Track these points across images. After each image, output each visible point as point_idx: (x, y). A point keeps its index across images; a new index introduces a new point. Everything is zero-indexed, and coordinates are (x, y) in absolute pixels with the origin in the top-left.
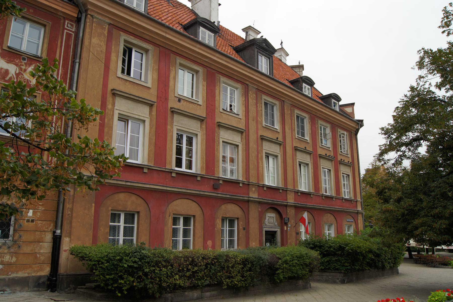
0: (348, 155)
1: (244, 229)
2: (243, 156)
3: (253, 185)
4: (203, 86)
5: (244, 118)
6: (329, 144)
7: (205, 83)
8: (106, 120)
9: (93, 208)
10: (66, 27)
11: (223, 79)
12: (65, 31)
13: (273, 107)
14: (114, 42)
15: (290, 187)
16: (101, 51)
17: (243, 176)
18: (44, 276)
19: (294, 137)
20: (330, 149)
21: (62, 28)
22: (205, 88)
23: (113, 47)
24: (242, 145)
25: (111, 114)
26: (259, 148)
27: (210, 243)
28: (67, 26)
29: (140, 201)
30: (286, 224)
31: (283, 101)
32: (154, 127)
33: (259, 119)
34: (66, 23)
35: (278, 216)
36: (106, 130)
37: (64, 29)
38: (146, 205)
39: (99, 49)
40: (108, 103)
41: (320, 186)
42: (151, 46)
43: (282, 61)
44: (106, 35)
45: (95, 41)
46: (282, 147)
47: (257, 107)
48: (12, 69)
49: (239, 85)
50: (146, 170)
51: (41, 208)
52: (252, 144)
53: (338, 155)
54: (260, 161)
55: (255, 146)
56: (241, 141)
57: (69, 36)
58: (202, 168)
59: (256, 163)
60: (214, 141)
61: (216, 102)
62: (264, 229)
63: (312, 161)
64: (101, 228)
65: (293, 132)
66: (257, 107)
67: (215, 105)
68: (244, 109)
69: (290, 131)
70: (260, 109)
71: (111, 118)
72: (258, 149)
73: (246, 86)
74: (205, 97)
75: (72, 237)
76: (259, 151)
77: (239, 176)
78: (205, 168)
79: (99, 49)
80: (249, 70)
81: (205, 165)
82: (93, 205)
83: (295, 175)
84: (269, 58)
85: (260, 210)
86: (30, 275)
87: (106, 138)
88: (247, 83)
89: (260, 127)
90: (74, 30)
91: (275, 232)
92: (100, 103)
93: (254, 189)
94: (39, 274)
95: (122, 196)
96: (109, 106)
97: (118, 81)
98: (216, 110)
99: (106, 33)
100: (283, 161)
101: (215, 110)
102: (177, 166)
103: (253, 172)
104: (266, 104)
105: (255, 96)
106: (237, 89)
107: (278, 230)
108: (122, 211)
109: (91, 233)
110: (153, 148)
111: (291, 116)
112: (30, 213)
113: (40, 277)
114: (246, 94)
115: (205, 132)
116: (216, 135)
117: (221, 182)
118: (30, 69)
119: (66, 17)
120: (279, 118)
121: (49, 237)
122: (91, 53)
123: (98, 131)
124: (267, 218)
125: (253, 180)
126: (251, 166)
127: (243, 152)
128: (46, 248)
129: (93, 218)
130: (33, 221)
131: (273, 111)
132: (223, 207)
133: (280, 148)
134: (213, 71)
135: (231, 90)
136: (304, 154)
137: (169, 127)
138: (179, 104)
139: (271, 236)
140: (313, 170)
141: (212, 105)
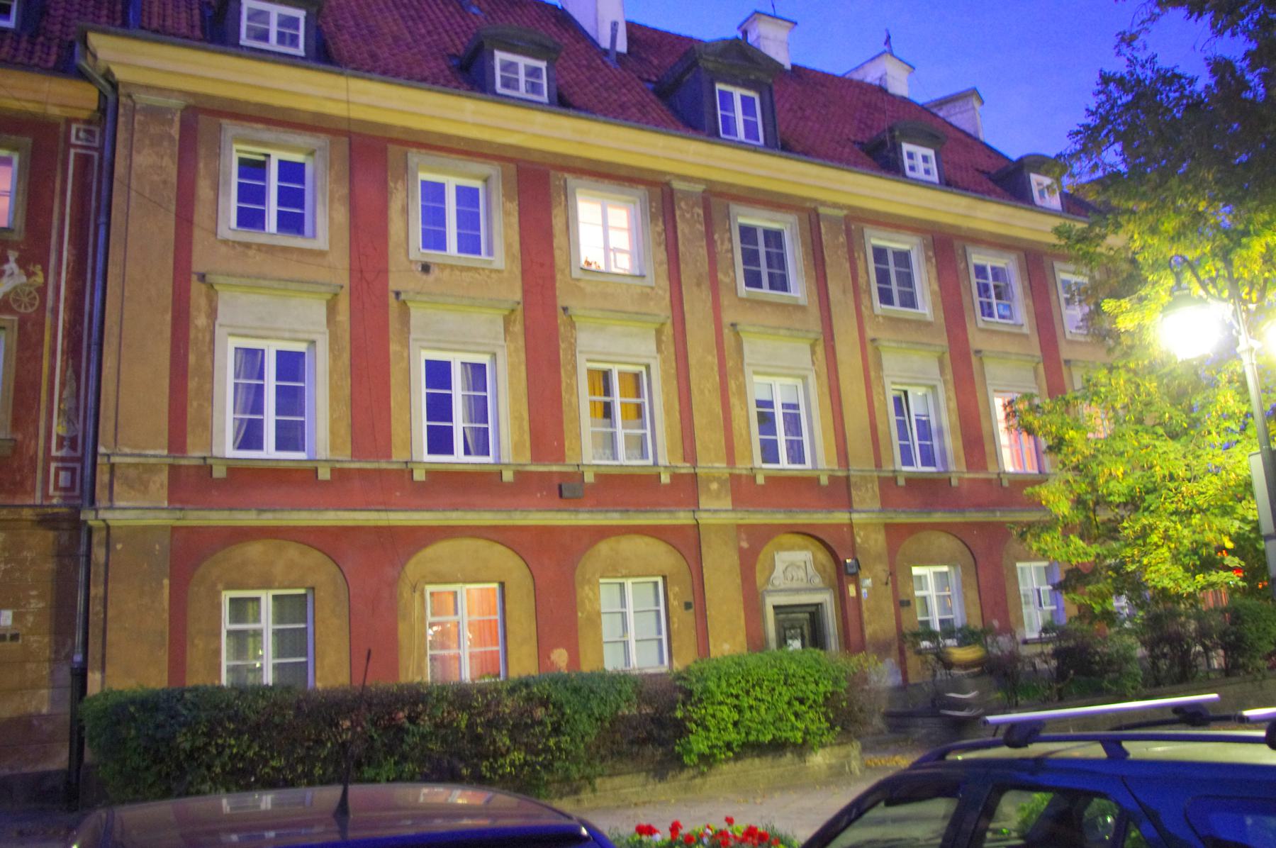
1: (688, 606)
4: (507, 214)
5: (665, 283)
7: (513, 207)
8: (192, 359)
9: (166, 591)
10: (73, 140)
12: (72, 151)
14: (202, 151)
16: (165, 182)
17: (671, 452)
18: (57, 773)
20: (1026, 330)
21: (62, 145)
22: (515, 220)
23: (201, 165)
24: (664, 361)
25: (208, 338)
26: (730, 364)
28: (77, 137)
29: (315, 557)
30: (855, 578)
32: (346, 356)
33: (721, 276)
34: (74, 132)
36: (192, 384)
37: (69, 145)
38: (334, 568)
39: (156, 178)
40: (193, 312)
42: (322, 136)
43: (891, 90)
44: (177, 137)
45: (143, 159)
47: (711, 244)
51: (35, 605)
54: (734, 401)
55: (712, 359)
56: (659, 350)
57: (84, 162)
58: (517, 447)
59: (718, 409)
60: (555, 365)
61: (557, 253)
62: (771, 601)
63: (949, 377)
64: (196, 641)
66: (711, 244)
67: (552, 266)
68: (662, 255)
70: (727, 245)
71: (205, 349)
74: (516, 246)
75: (109, 670)
78: (528, 444)
79: (156, 178)
81: (527, 437)
82: (166, 582)
85: (745, 545)
86: (16, 772)
87: (195, 404)
89: (725, 300)
90: (96, 144)
92: (168, 317)
94: (40, 768)
95: (255, 550)
96: (200, 321)
97: (224, 249)
98: (559, 277)
99: (175, 131)
100: (826, 390)
102: (432, 451)
105: (701, 212)
107: (825, 598)
109: (164, 656)
110: (345, 410)
111: (851, 252)
113: (45, 775)
115: (521, 343)
116: (562, 346)
120: (801, 265)
122: (133, 194)
123: (167, 391)
126: (699, 420)
129: (166, 616)
130: (15, 637)
137: (394, 347)
138: (424, 277)
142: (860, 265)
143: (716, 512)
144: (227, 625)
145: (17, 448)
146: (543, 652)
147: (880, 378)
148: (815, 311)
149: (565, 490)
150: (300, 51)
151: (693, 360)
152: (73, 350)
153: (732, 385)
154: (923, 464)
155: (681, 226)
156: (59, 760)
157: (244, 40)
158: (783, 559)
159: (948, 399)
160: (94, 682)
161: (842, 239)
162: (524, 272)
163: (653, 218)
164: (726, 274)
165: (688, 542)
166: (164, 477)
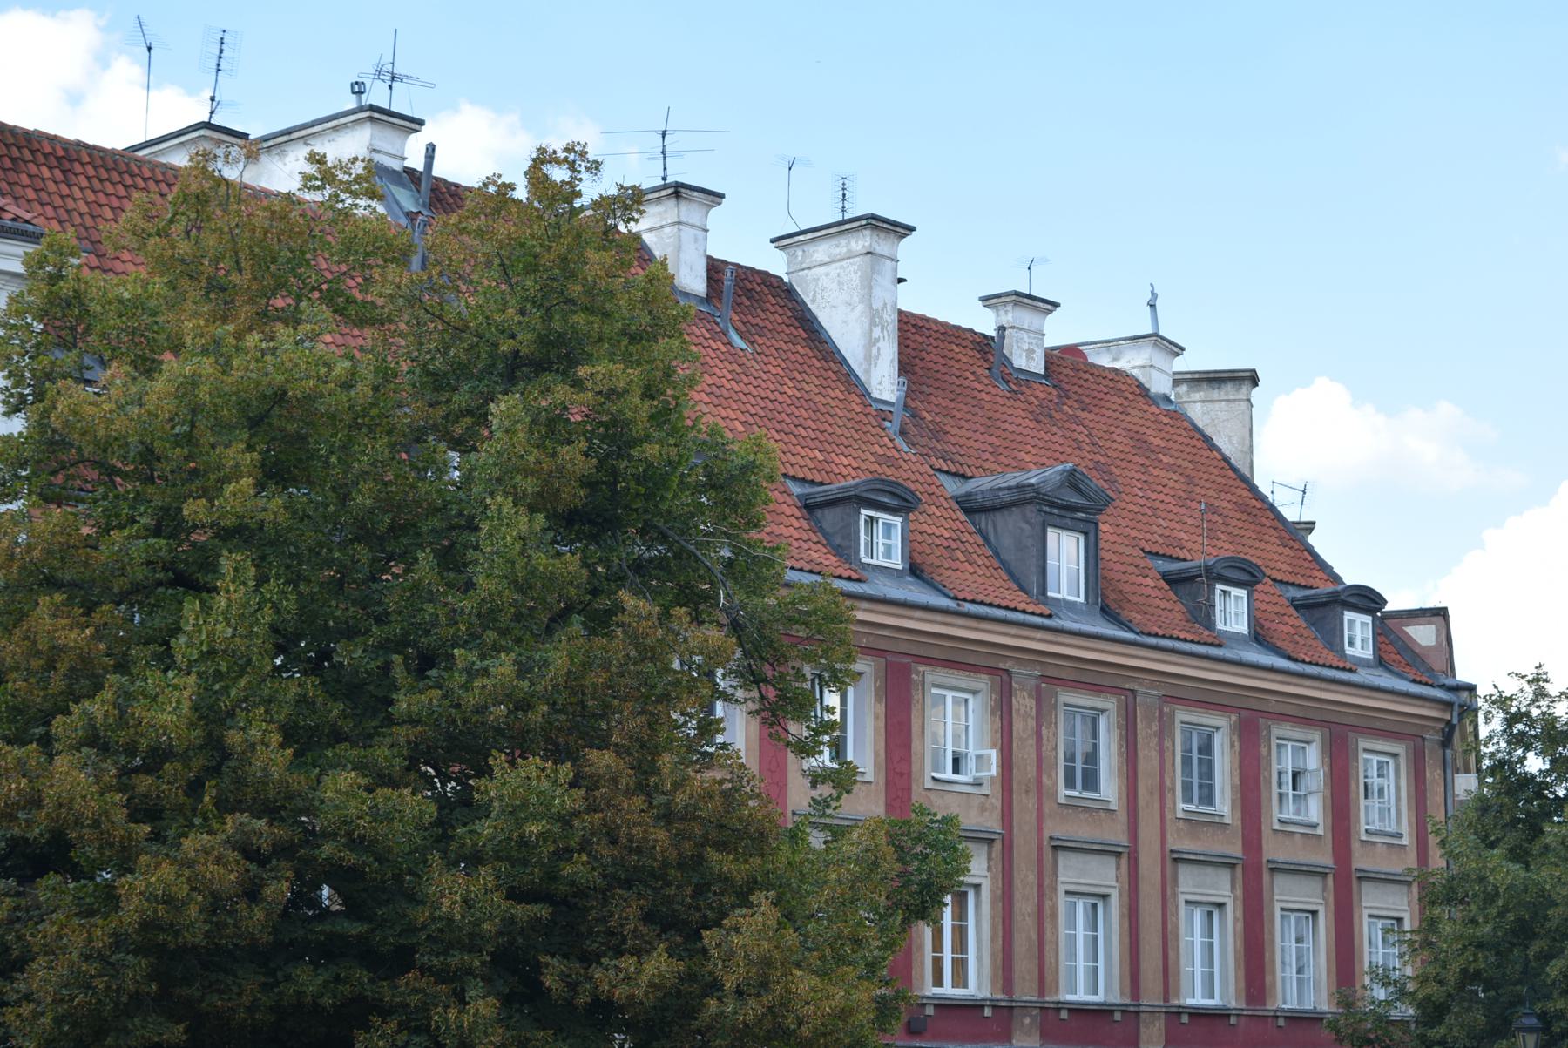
0: (1400, 836)
2: (993, 918)
4: (876, 717)
6: (1315, 811)
7: (881, 708)
11: (932, 675)
13: (1095, 721)
15: (1151, 997)
19: (1169, 816)
20: (1320, 831)
22: (882, 724)
24: (992, 884)
26: (1047, 882)
31: (1133, 691)
33: (1045, 779)
41: (1268, 979)
46: (1124, 861)
49: (982, 682)
52: (1025, 875)
53: (1355, 846)
54: (1048, 926)
55: (1032, 878)
56: (989, 869)
59: (1035, 936)
63: (1239, 892)
65: (1169, 796)
69: (1157, 797)
72: (1040, 886)
73: (1005, 677)
76: (1044, 891)
77: (978, 986)
80: (1013, 631)
83: (1171, 954)
84: (1086, 534)
88: (1008, 665)
89: (1048, 807)
93: (1027, 1021)
98: (914, 787)
100: (1126, 911)
101: (909, 789)
103: (1024, 967)
104: (1069, 716)
106: (974, 693)
114: (1003, 709)
117: (930, 1011)
125: (1026, 993)
127: (993, 903)
131: (1095, 735)
133: (1118, 868)
134: (905, 660)
135: (956, 701)
136: (1209, 870)
140: (1240, 925)
141: (902, 775)
142: (1167, 755)
147: (1175, 895)
148: (1122, 817)
151: (1017, 883)
153: (1048, 904)
154: (1203, 997)
159: (1236, 919)
161: (1155, 727)
162: (888, 783)
163: (993, 713)
164: (1050, 776)
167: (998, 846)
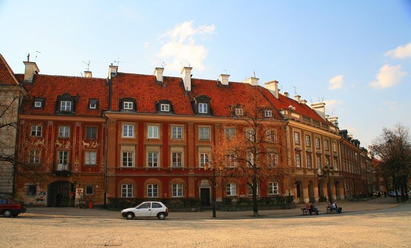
3: (191, 169)
27: (166, 194)
29: (132, 180)
30: (215, 185)
35: (210, 181)
48: (88, 145)
50: (134, 170)
58: (161, 165)
85: (196, 179)
91: (209, 189)
95: (125, 179)
107: (210, 188)
108: (127, 184)
112: (97, 186)
118: (93, 143)
119: (103, 123)
121: (103, 193)
124: (202, 183)
128: (103, 196)
132: (173, 179)
139: (205, 191)
143: (191, 173)
144: (122, 188)
145: (98, 166)
146: (163, 193)
149: (168, 171)
150: (132, 109)
152: (104, 153)
155: (189, 130)
156: (103, 203)
157: (124, 108)
158: (203, 182)
160: (107, 194)
165: (186, 179)
166: (114, 170)
167: (186, 147)
